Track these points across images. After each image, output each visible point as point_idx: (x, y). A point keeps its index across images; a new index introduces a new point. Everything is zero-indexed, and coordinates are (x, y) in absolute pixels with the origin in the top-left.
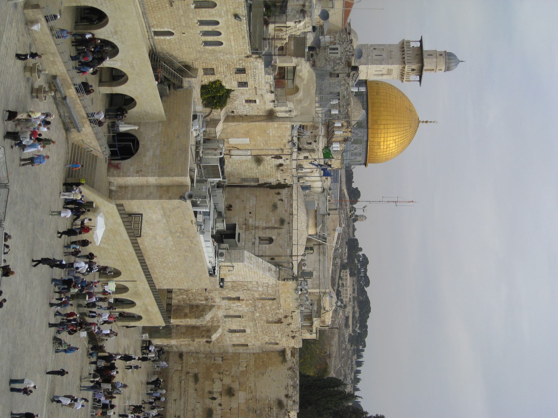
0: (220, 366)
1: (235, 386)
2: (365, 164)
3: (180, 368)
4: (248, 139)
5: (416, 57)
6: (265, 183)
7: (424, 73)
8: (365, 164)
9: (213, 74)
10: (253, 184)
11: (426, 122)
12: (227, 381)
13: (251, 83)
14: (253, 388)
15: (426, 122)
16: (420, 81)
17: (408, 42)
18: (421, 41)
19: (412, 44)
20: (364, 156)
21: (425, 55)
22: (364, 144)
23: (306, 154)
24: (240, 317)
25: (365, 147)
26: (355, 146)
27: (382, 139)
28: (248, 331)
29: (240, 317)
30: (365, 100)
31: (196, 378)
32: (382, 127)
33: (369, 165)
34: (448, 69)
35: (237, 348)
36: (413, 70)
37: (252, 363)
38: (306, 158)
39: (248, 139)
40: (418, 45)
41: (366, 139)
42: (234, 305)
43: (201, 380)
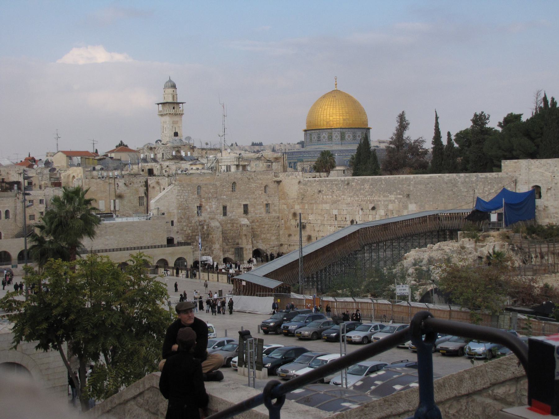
0: (285, 222)
1: (292, 211)
2: (369, 129)
3: (286, 246)
4: (100, 201)
5: (172, 107)
6: (145, 193)
7: (178, 101)
8: (369, 129)
9: (34, 215)
10: (145, 199)
11: (336, 85)
12: (291, 217)
13: (41, 198)
14: (292, 200)
15: (336, 85)
16: (182, 103)
17: (160, 112)
18: (158, 104)
19: (161, 109)
20: (356, 130)
21: (165, 101)
22: (344, 130)
23: (164, 171)
24: (225, 208)
25: (347, 130)
26: (347, 137)
27: (341, 117)
28: (245, 203)
29: (225, 208)
30: (313, 131)
31: (290, 235)
32: (331, 118)
33: (369, 126)
34: (174, 86)
35: (271, 210)
36: (174, 108)
37: (283, 201)
38: (166, 171)
39: (100, 201)
40: (160, 105)
41: (340, 130)
42: (209, 210)
43: (291, 233)
